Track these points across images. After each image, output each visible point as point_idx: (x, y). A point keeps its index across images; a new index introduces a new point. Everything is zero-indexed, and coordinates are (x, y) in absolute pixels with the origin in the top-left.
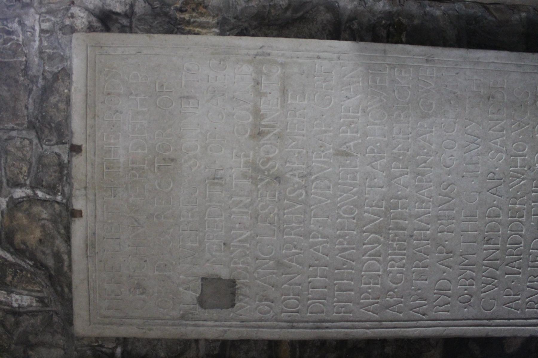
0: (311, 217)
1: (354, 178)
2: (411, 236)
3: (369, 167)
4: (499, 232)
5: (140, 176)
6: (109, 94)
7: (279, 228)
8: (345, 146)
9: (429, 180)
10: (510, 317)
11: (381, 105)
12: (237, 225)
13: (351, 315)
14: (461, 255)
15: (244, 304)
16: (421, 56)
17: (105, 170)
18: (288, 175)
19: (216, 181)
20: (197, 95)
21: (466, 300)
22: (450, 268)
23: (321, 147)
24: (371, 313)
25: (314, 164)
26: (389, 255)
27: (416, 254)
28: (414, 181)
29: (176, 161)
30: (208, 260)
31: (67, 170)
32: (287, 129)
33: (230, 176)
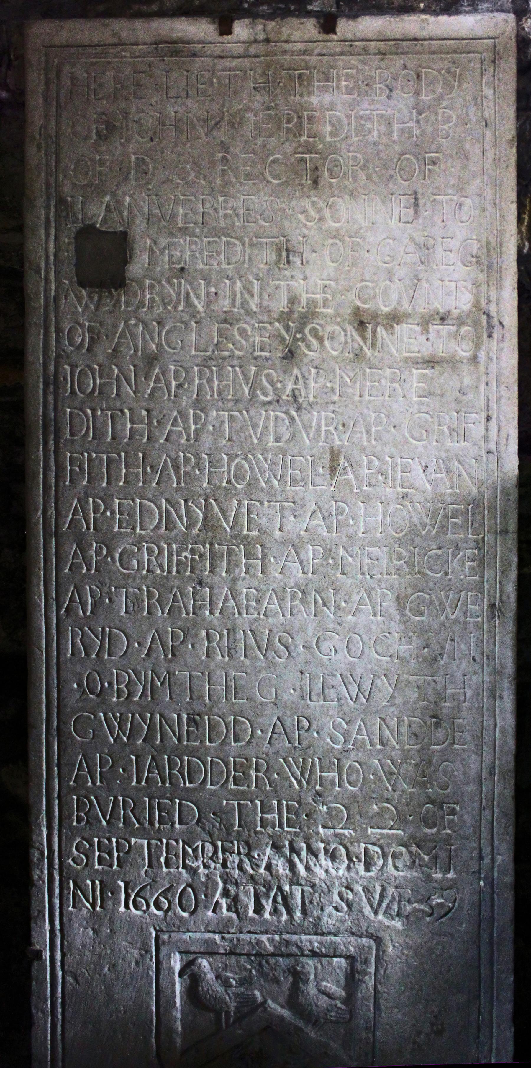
0: (229, 411)
1: (294, 482)
2: (200, 583)
3: (314, 507)
4: (210, 742)
5: (288, 129)
6: (419, 76)
7: (211, 358)
8: (346, 465)
9: (295, 611)
10: (63, 767)
11: (416, 526)
12: (213, 290)
13: (67, 483)
14: (168, 673)
15: (84, 302)
16: (501, 595)
17: (297, 72)
18: (296, 371)
19: (284, 254)
20: (421, 221)
21: (91, 685)
22: (148, 655)
23: (344, 425)
24: (70, 517)
25: (315, 414)
26: (169, 544)
27: (171, 592)
28: (293, 584)
29: (315, 188)
30: (155, 243)
31: (295, 10)
32: (370, 368)
33: (292, 277)
